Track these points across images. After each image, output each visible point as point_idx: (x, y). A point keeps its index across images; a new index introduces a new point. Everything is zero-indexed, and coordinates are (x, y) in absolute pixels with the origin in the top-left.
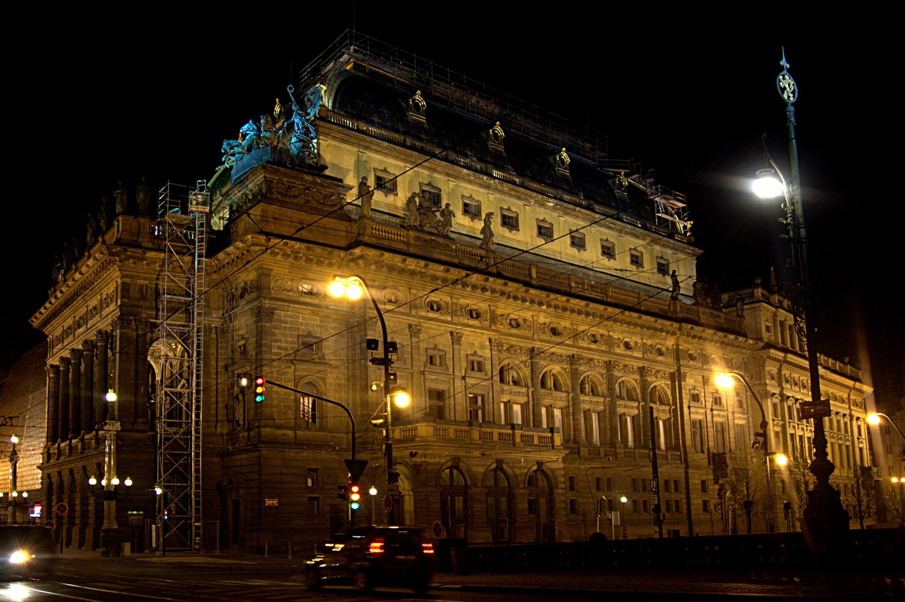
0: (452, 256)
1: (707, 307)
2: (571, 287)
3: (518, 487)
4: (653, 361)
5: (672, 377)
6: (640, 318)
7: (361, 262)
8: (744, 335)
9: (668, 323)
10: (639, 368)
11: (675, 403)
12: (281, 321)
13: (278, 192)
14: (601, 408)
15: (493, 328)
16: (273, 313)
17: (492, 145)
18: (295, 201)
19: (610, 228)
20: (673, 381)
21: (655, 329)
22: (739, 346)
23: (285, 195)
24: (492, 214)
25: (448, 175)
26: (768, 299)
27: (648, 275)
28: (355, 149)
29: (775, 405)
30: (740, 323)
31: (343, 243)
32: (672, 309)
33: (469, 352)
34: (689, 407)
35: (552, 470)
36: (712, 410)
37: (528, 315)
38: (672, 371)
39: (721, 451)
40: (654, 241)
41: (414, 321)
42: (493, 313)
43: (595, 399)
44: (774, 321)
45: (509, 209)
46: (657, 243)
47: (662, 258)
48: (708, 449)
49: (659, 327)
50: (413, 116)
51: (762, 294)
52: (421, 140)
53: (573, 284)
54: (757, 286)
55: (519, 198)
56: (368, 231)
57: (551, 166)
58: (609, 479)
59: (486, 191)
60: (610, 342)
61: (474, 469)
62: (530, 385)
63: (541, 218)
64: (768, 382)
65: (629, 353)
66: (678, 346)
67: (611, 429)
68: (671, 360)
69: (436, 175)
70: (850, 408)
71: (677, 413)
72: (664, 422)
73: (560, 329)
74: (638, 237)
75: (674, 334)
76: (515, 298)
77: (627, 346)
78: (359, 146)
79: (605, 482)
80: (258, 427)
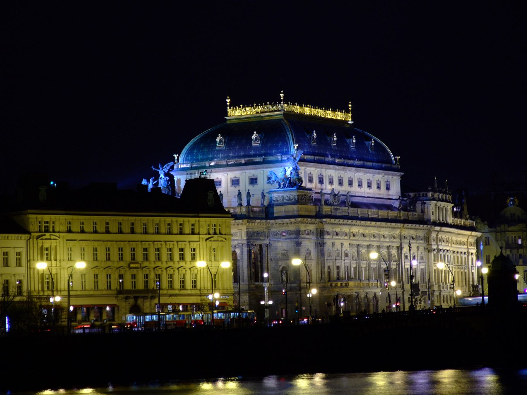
1: (411, 211)
4: (393, 242)
5: (398, 248)
11: (399, 261)
14: (376, 266)
20: (398, 250)
27: (383, 193)
29: (434, 255)
30: (423, 215)
37: (357, 231)
41: (333, 241)
44: (436, 208)
54: (429, 191)
59: (334, 171)
64: (432, 243)
66: (401, 233)
68: (397, 240)
69: (323, 170)
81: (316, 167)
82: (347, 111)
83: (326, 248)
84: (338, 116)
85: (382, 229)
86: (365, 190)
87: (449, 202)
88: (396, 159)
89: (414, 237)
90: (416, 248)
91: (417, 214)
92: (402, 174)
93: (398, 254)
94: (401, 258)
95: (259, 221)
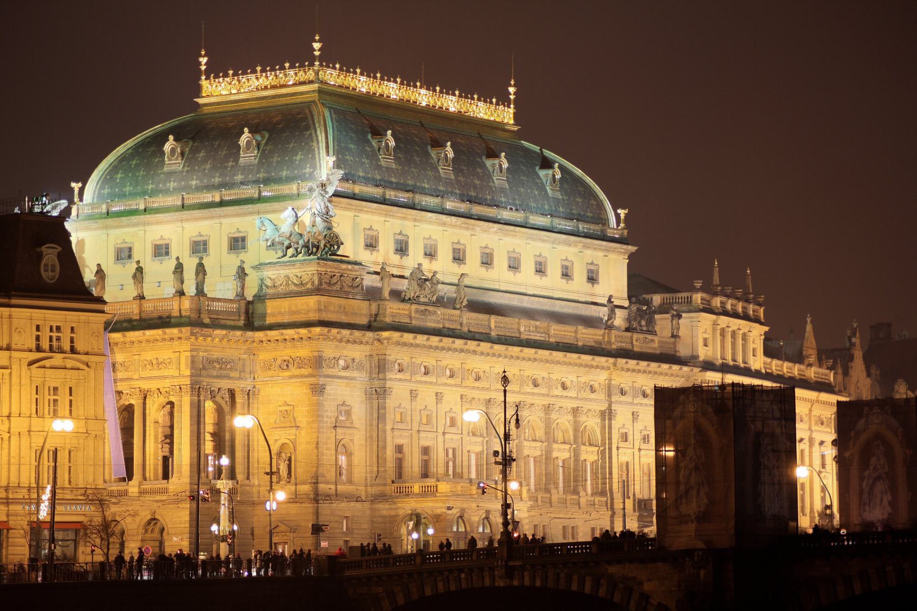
1: (642, 332)
4: (586, 399)
5: (603, 413)
6: (579, 358)
10: (573, 408)
11: (604, 444)
14: (538, 453)
15: (464, 384)
18: (335, 288)
19: (544, 241)
20: (603, 419)
22: (672, 375)
24: (467, 275)
25: (415, 220)
27: (578, 287)
30: (674, 343)
32: (606, 339)
34: (618, 448)
36: (640, 450)
39: (646, 497)
40: (586, 247)
41: (413, 386)
43: (534, 444)
44: (714, 330)
48: (634, 495)
51: (702, 299)
53: (522, 329)
54: (697, 290)
56: (389, 311)
59: (441, 228)
60: (549, 383)
62: (485, 435)
65: (565, 393)
66: (610, 380)
67: (546, 474)
69: (406, 223)
70: (810, 429)
71: (606, 453)
74: (570, 245)
75: (609, 368)
77: (564, 387)
82: (504, 100)
84: (481, 110)
87: (756, 320)
91: (656, 339)
93: (603, 427)
94: (610, 439)
95: (224, 332)
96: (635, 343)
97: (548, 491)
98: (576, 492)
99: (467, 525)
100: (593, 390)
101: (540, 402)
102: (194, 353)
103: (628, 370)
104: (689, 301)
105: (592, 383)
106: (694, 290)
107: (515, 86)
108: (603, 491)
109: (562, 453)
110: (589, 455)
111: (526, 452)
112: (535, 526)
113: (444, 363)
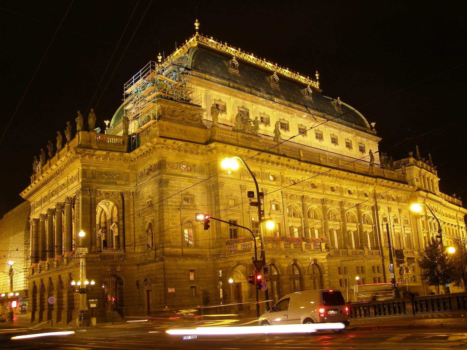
0: (260, 146)
1: (388, 169)
2: (320, 161)
3: (305, 275)
5: (373, 208)
6: (356, 176)
7: (214, 151)
8: (407, 184)
9: (370, 179)
12: (172, 187)
13: (168, 114)
14: (339, 228)
16: (168, 182)
17: (272, 85)
18: (177, 118)
19: (335, 128)
20: (373, 211)
21: (364, 183)
22: (405, 190)
23: (172, 116)
25: (252, 102)
26: (416, 163)
27: (355, 153)
28: (204, 89)
29: (423, 222)
30: (404, 177)
31: (203, 141)
33: (271, 200)
35: (322, 264)
36: (394, 226)
38: (373, 205)
39: (399, 249)
40: (357, 135)
42: (282, 177)
43: (335, 223)
45: (284, 119)
46: (358, 135)
47: (361, 143)
49: (366, 181)
50: (232, 71)
51: (413, 161)
52: (236, 83)
53: (321, 159)
55: (288, 113)
56: (217, 133)
57: (302, 96)
58: (345, 267)
59: (271, 110)
60: (341, 190)
61: (283, 265)
62: (302, 217)
63: (300, 124)
65: (351, 196)
66: (375, 191)
67: (344, 239)
70: (457, 222)
72: (370, 234)
73: (316, 185)
74: (348, 132)
75: (373, 184)
76: (294, 168)
77: (349, 192)
78: (206, 87)
79: (343, 269)
80: (163, 247)
81: (230, 95)
82: (313, 78)
83: (222, 192)
85: (345, 182)
86: (326, 144)
88: (371, 126)
89: (395, 198)
90: (397, 211)
92: (380, 139)
93: (374, 215)
94: (378, 220)
96: (385, 174)
97: (346, 248)
98: (362, 248)
99: (279, 270)
100: (366, 195)
101: (337, 200)
102: (85, 168)
103: (383, 186)
104: (408, 162)
105: (365, 192)
106: (409, 156)
107: (318, 73)
108: (377, 247)
109: (352, 228)
110: (368, 229)
111: (330, 227)
112: (339, 268)
113: (267, 171)
